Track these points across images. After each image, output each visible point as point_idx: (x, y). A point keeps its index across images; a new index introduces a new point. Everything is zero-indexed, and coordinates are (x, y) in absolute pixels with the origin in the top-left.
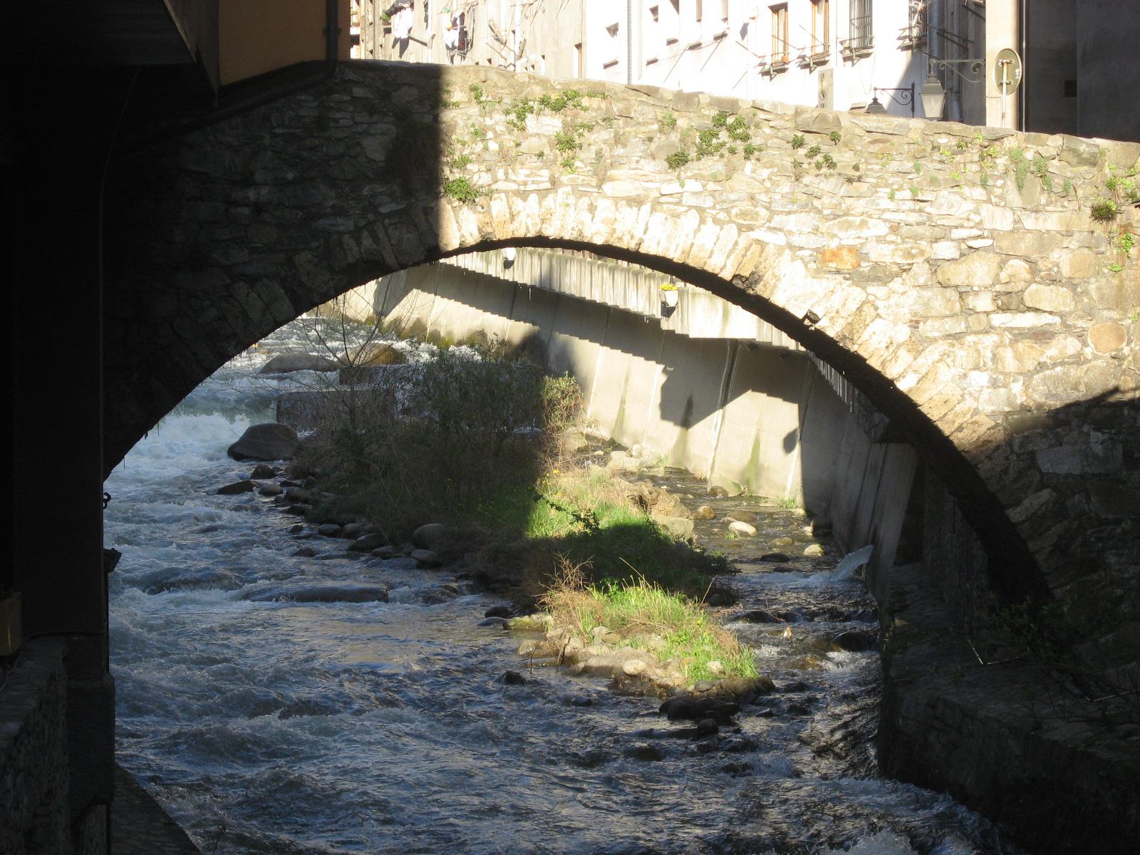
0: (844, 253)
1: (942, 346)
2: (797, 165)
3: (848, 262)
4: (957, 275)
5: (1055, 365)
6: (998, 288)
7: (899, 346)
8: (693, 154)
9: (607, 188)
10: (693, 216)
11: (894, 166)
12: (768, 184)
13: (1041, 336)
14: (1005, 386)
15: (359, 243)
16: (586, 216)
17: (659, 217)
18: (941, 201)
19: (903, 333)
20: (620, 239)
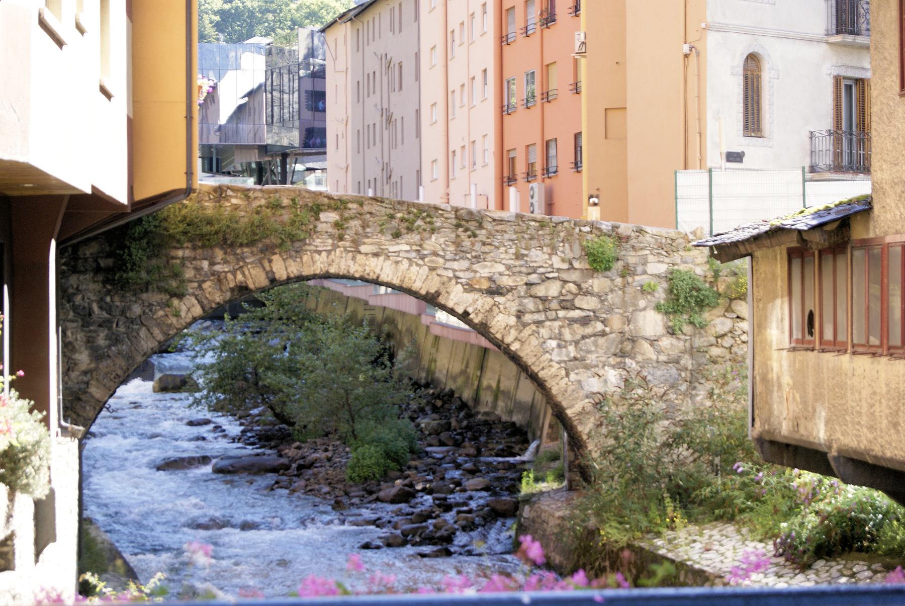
0: (483, 280)
1: (534, 327)
2: (458, 236)
3: (485, 285)
4: (540, 291)
5: (591, 336)
6: (562, 298)
7: (511, 327)
8: (404, 231)
9: (363, 249)
10: (406, 263)
11: (507, 236)
12: (443, 246)
13: (585, 321)
14: (565, 347)
15: (235, 278)
16: (351, 263)
17: (388, 263)
18: (531, 254)
19: (513, 320)
20: (368, 274)
